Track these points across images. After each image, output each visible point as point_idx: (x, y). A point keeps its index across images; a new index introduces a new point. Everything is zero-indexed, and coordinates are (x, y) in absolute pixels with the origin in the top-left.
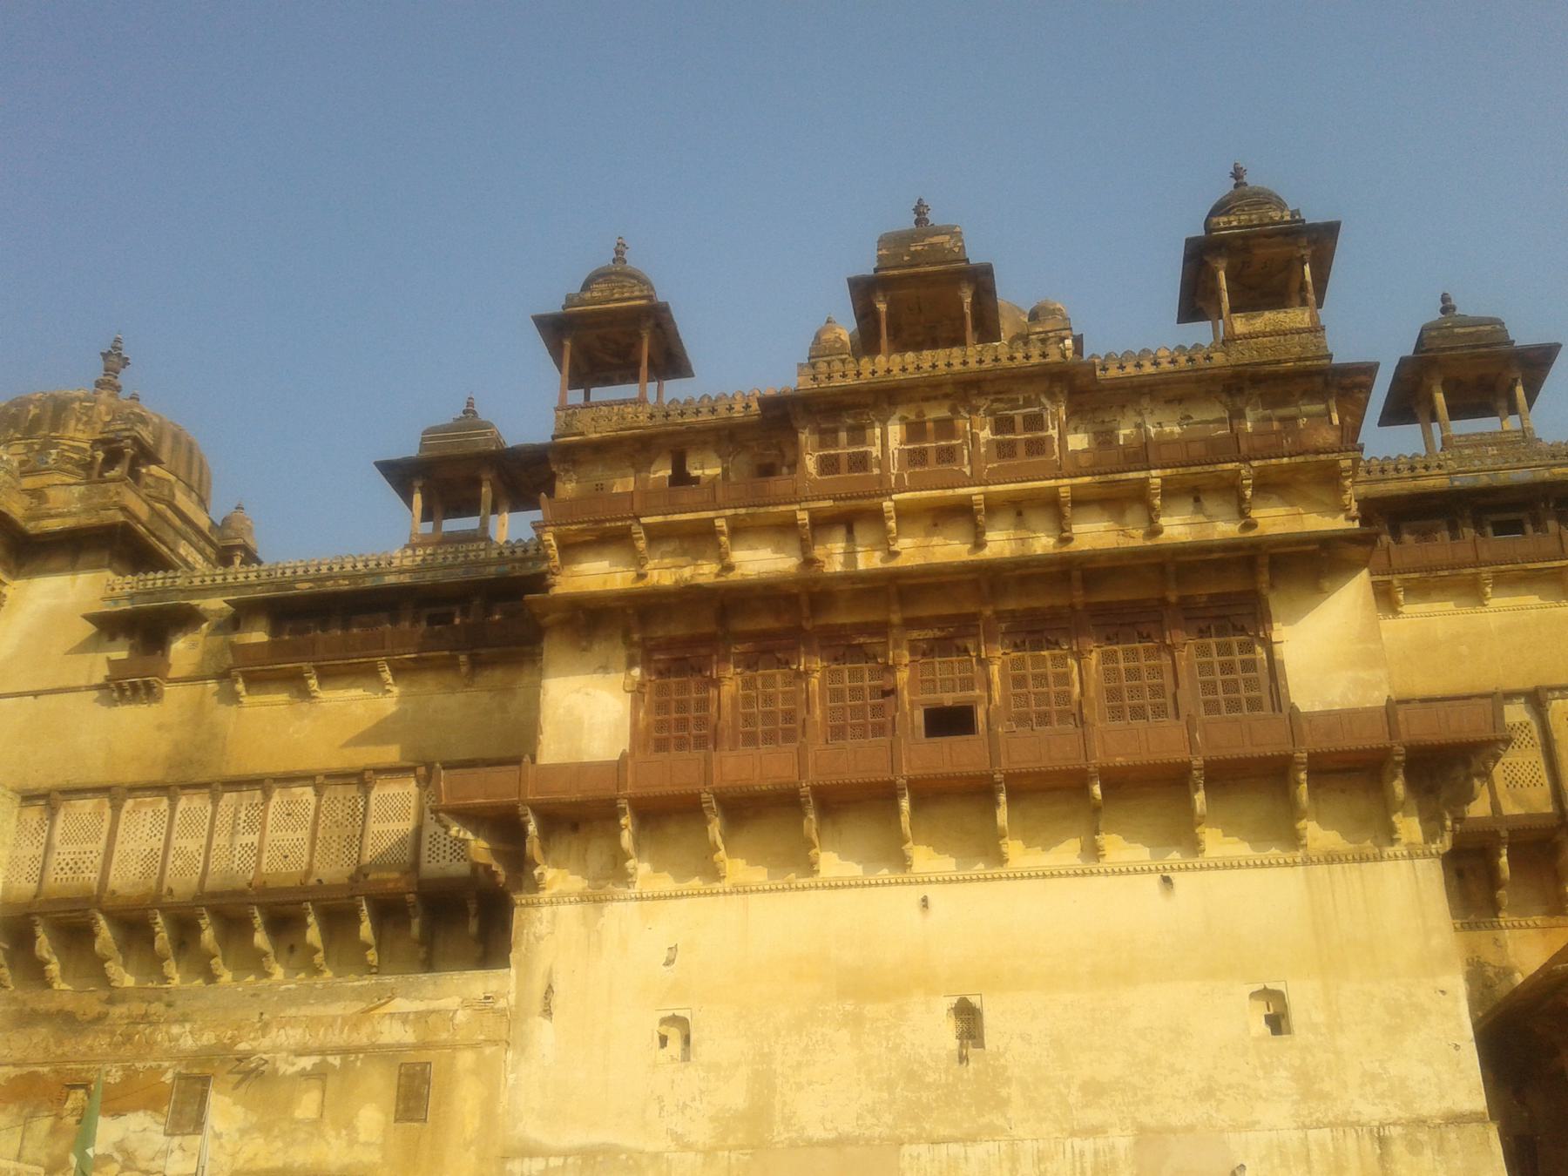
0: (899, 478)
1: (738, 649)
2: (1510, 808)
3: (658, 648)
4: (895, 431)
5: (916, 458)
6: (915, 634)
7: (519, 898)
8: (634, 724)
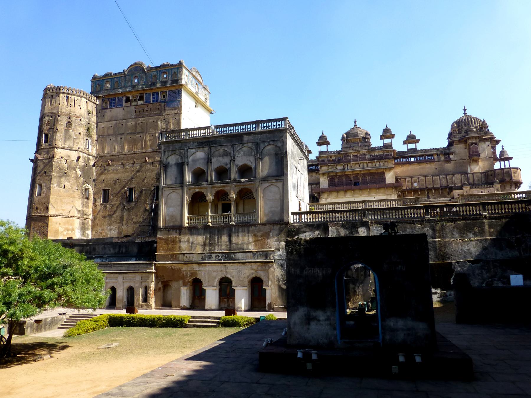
1: (338, 177)
2: (407, 188)
6: (354, 175)
7: (320, 199)
8: (328, 184)
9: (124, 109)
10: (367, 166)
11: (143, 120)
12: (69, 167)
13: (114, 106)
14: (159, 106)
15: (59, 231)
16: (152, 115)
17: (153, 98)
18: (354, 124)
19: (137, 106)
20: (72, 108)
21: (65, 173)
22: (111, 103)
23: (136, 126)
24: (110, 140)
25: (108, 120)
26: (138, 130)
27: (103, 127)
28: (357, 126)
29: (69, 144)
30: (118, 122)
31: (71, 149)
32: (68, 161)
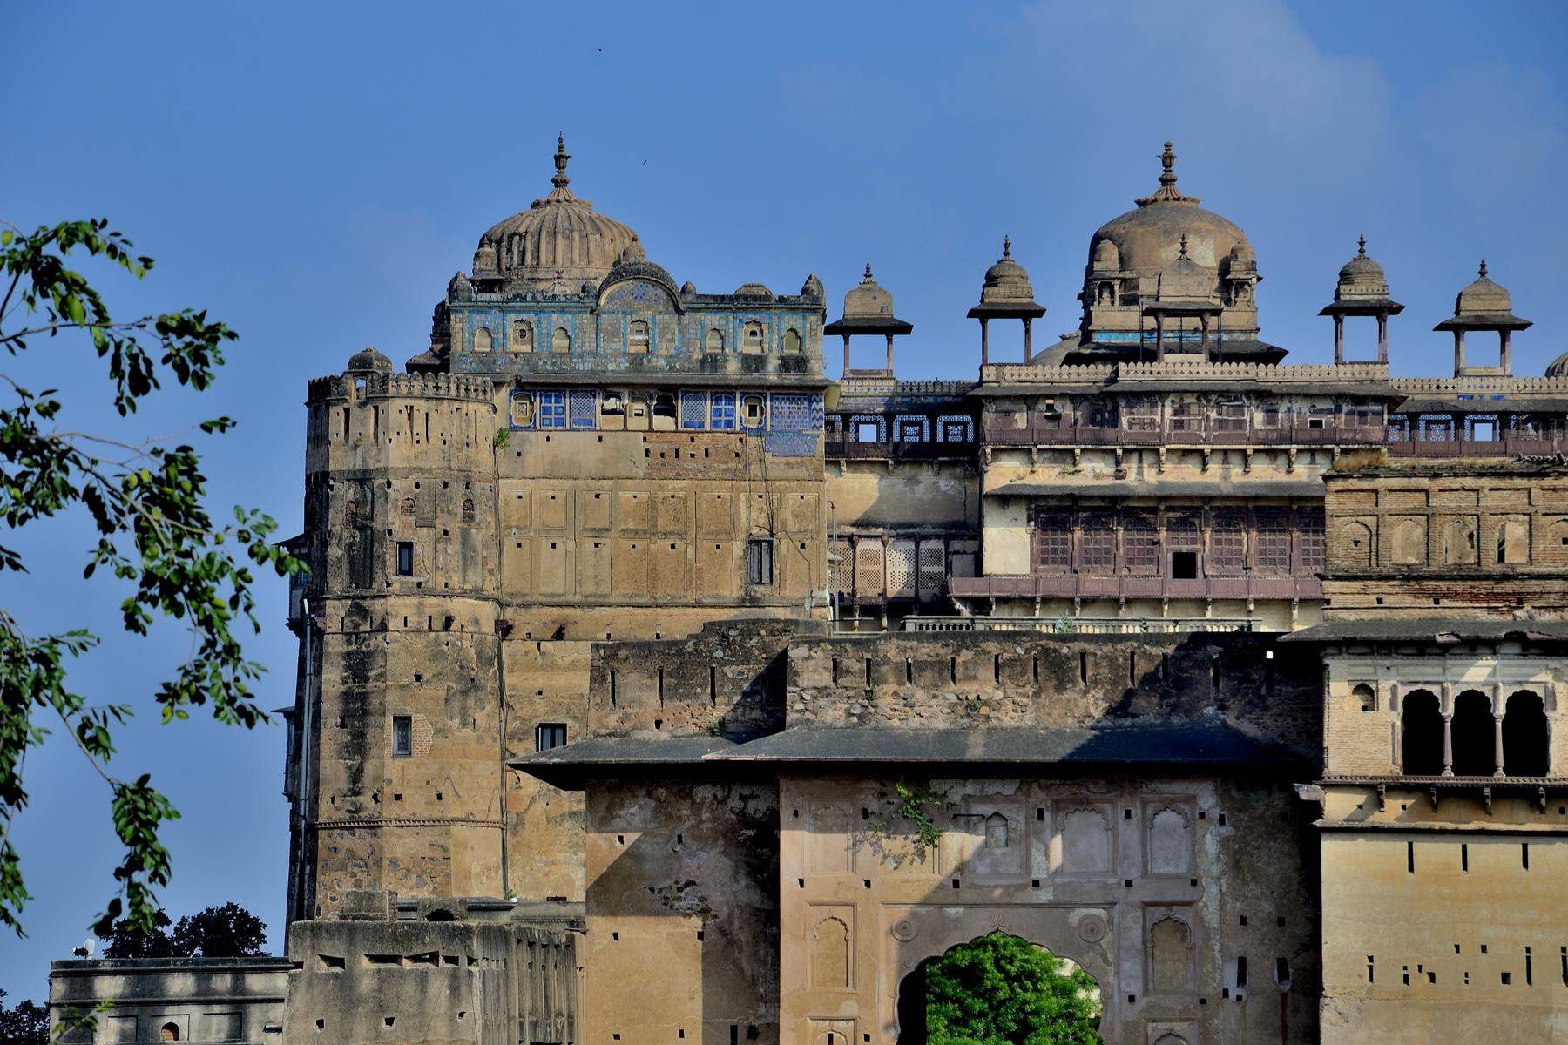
0: (1169, 435)
1: (1083, 515)
3: (1043, 511)
4: (1168, 411)
5: (1178, 425)
6: (1171, 515)
9: (600, 439)
11: (682, 489)
12: (480, 656)
13: (561, 422)
14: (739, 444)
15: (474, 872)
16: (712, 475)
17: (717, 412)
18: (1160, 171)
19: (654, 435)
20: (472, 450)
21: (473, 680)
22: (546, 411)
23: (655, 508)
24: (554, 546)
25: (539, 473)
26: (663, 523)
27: (520, 497)
29: (474, 580)
30: (579, 483)
31: (478, 594)
32: (476, 636)
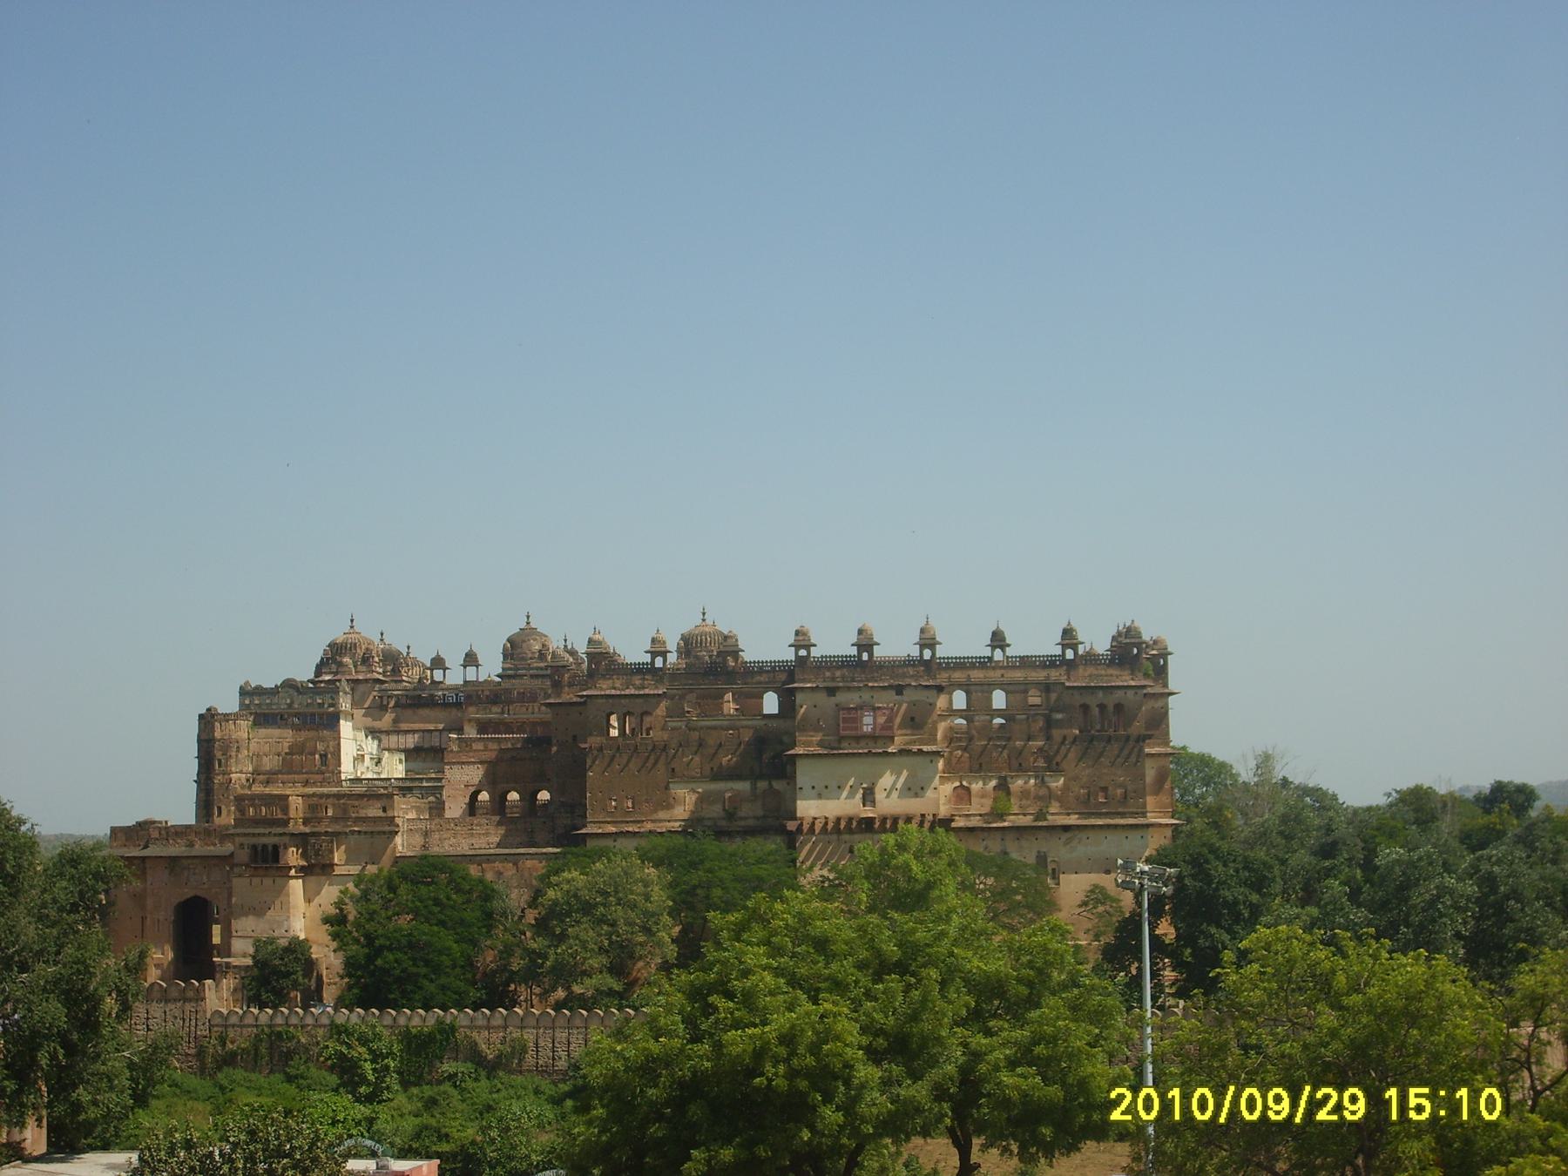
10: (539, 709)
22: (264, 720)
28: (533, 625)
31: (241, 772)
